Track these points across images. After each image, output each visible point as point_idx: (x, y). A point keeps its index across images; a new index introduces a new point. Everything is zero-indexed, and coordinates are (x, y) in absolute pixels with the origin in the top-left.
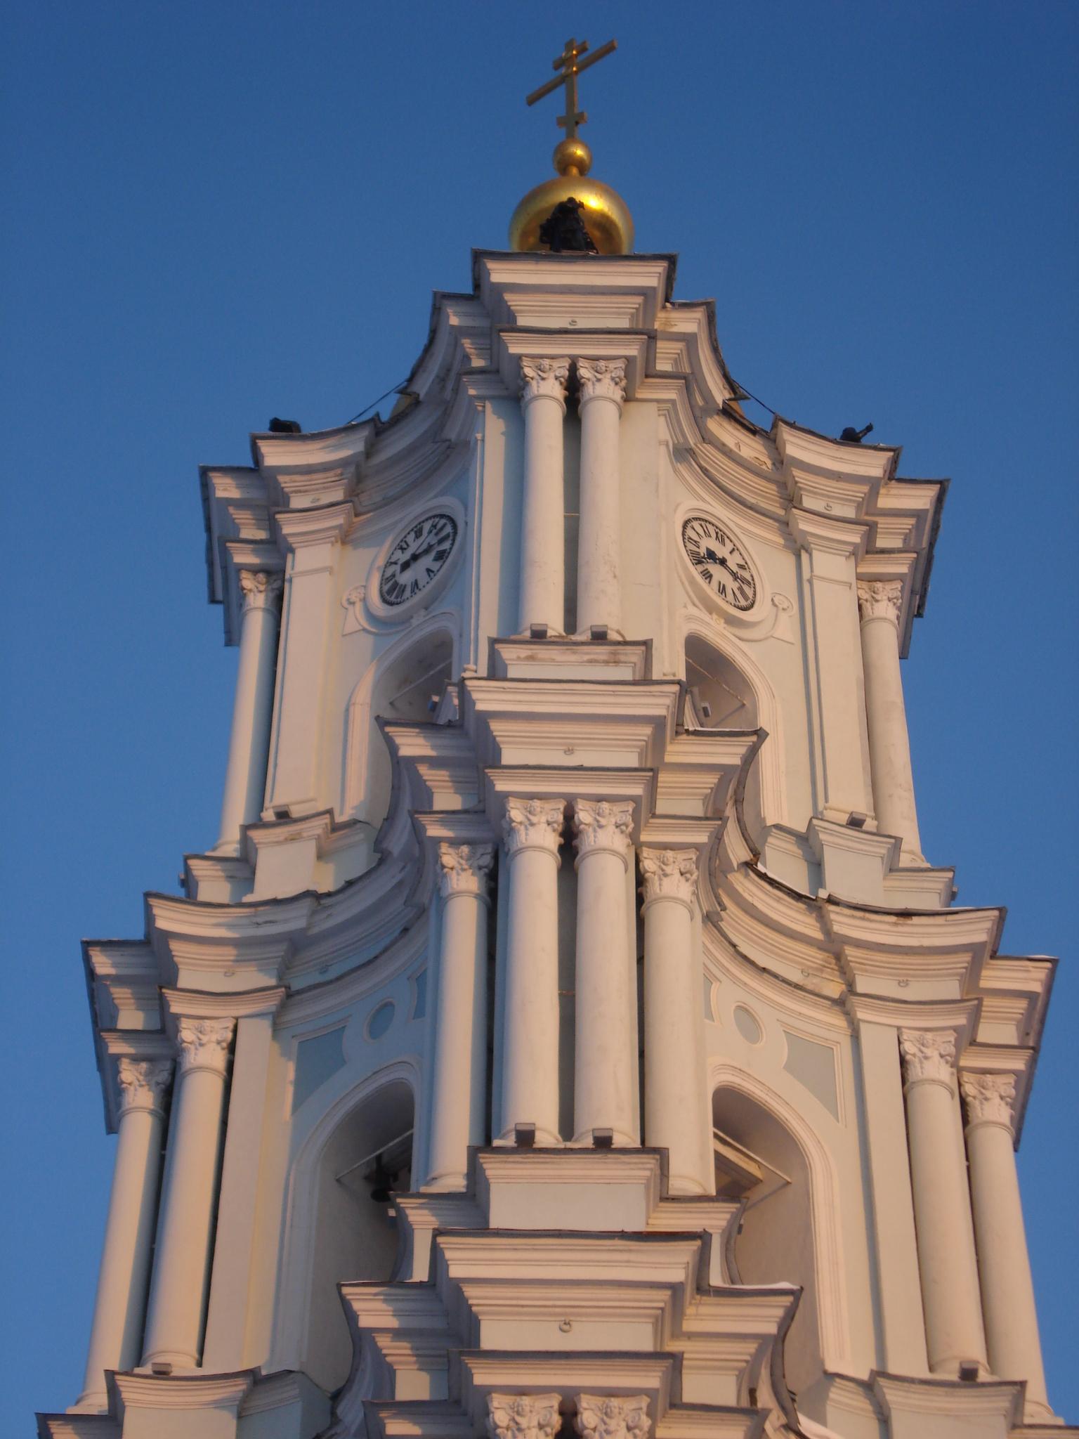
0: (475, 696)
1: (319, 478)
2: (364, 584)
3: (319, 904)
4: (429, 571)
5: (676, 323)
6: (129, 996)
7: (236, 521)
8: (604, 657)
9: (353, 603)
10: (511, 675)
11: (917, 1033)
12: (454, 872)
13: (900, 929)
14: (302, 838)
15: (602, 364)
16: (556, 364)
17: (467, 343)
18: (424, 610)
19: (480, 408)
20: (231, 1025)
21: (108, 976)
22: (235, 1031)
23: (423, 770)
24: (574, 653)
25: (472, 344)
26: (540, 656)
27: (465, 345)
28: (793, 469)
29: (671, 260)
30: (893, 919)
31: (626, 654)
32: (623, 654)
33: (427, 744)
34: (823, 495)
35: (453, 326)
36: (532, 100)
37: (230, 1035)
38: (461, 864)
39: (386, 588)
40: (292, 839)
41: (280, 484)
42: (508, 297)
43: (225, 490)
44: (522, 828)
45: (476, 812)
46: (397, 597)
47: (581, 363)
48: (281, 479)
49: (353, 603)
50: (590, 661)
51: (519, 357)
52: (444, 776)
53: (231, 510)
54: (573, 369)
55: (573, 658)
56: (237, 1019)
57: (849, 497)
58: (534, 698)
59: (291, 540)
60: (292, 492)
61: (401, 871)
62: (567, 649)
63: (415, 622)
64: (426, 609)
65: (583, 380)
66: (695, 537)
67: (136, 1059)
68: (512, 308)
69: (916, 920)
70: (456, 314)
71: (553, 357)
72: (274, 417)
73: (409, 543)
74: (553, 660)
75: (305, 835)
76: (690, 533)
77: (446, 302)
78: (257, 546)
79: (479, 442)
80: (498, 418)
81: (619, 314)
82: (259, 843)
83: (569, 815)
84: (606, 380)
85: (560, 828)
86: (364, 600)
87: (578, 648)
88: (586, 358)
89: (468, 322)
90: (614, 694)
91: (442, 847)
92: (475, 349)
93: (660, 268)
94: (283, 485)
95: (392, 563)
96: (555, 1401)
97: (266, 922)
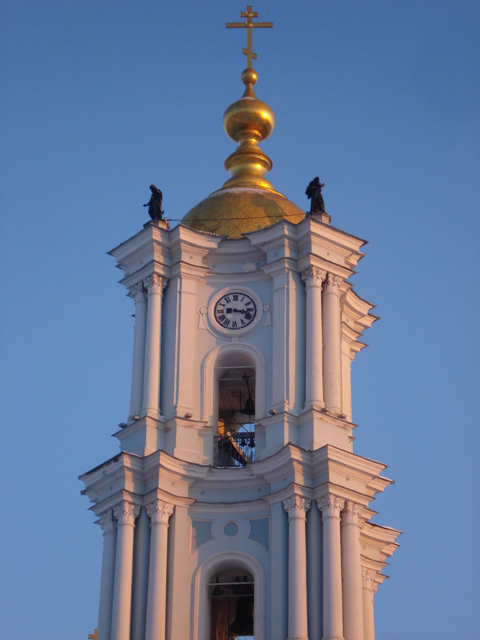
1: (195, 249)
2: (207, 307)
3: (211, 470)
4: (242, 321)
5: (352, 259)
6: (131, 476)
7: (154, 249)
8: (341, 425)
9: (203, 314)
11: (367, 569)
12: (298, 508)
13: (371, 530)
14: (193, 428)
15: (336, 278)
17: (286, 242)
18: (238, 338)
19: (286, 272)
20: (173, 507)
21: (127, 467)
23: (295, 464)
24: (334, 421)
25: (288, 243)
26: (324, 419)
27: (286, 242)
28: (344, 304)
29: (365, 242)
30: (370, 526)
31: (348, 427)
32: (348, 426)
33: (301, 455)
34: (348, 315)
35: (285, 234)
37: (172, 512)
38: (301, 505)
40: (189, 427)
41: (181, 246)
42: (312, 236)
43: (156, 236)
44: (333, 507)
45: (310, 488)
46: (224, 323)
48: (182, 244)
49: (203, 314)
50: (338, 426)
51: (312, 266)
52: (300, 467)
53: (155, 244)
55: (333, 423)
57: (354, 318)
58: (345, 458)
59: (182, 274)
60: (183, 250)
61: (250, 476)
62: (333, 419)
63: (232, 339)
64: (239, 337)
65: (329, 283)
67: (131, 503)
68: (312, 241)
69: (376, 528)
70: (288, 229)
71: (322, 269)
72: (152, 184)
73: (230, 300)
74: (327, 422)
75: (194, 427)
77: (286, 223)
78: (165, 267)
79: (285, 289)
80: (294, 281)
81: (342, 255)
82: (178, 424)
84: (337, 286)
86: (207, 314)
87: (336, 420)
88: (332, 273)
89: (291, 235)
90: (367, 463)
91: (297, 497)
92: (289, 245)
93: (361, 243)
94: (182, 247)
95: (221, 304)
97: (191, 471)
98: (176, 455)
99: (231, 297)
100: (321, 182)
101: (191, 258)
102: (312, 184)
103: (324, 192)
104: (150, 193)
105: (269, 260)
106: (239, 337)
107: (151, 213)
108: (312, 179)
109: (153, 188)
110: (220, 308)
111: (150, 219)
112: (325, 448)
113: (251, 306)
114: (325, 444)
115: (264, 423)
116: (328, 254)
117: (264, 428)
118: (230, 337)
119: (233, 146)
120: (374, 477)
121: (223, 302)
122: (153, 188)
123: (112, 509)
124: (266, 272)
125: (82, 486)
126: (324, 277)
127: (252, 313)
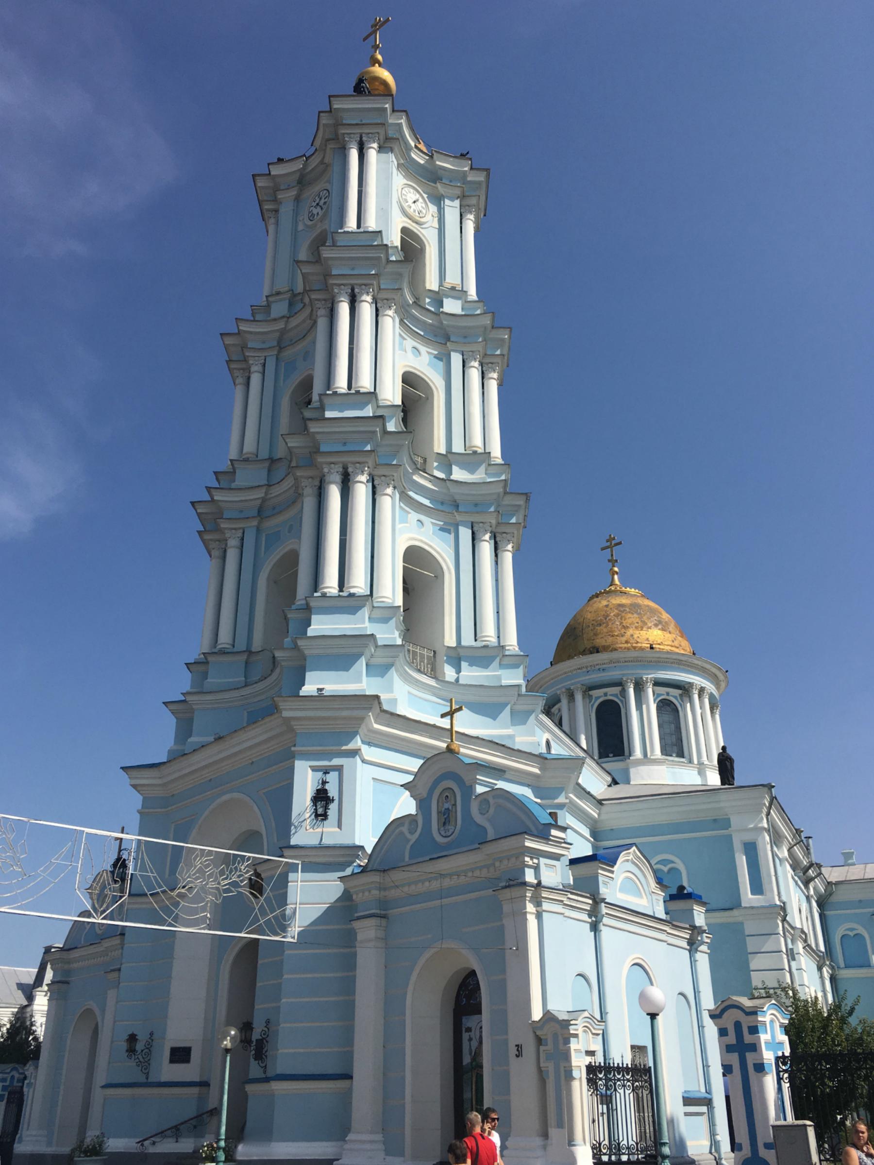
0: (323, 252)
10: (338, 244)
16: (356, 136)
22: (265, 360)
36: (365, 39)
39: (310, 215)
47: (363, 135)
54: (361, 137)
56: (265, 356)
63: (318, 226)
64: (321, 221)
66: (405, 193)
76: (404, 192)
83: (353, 290)
85: (350, 293)
96: (341, 465)
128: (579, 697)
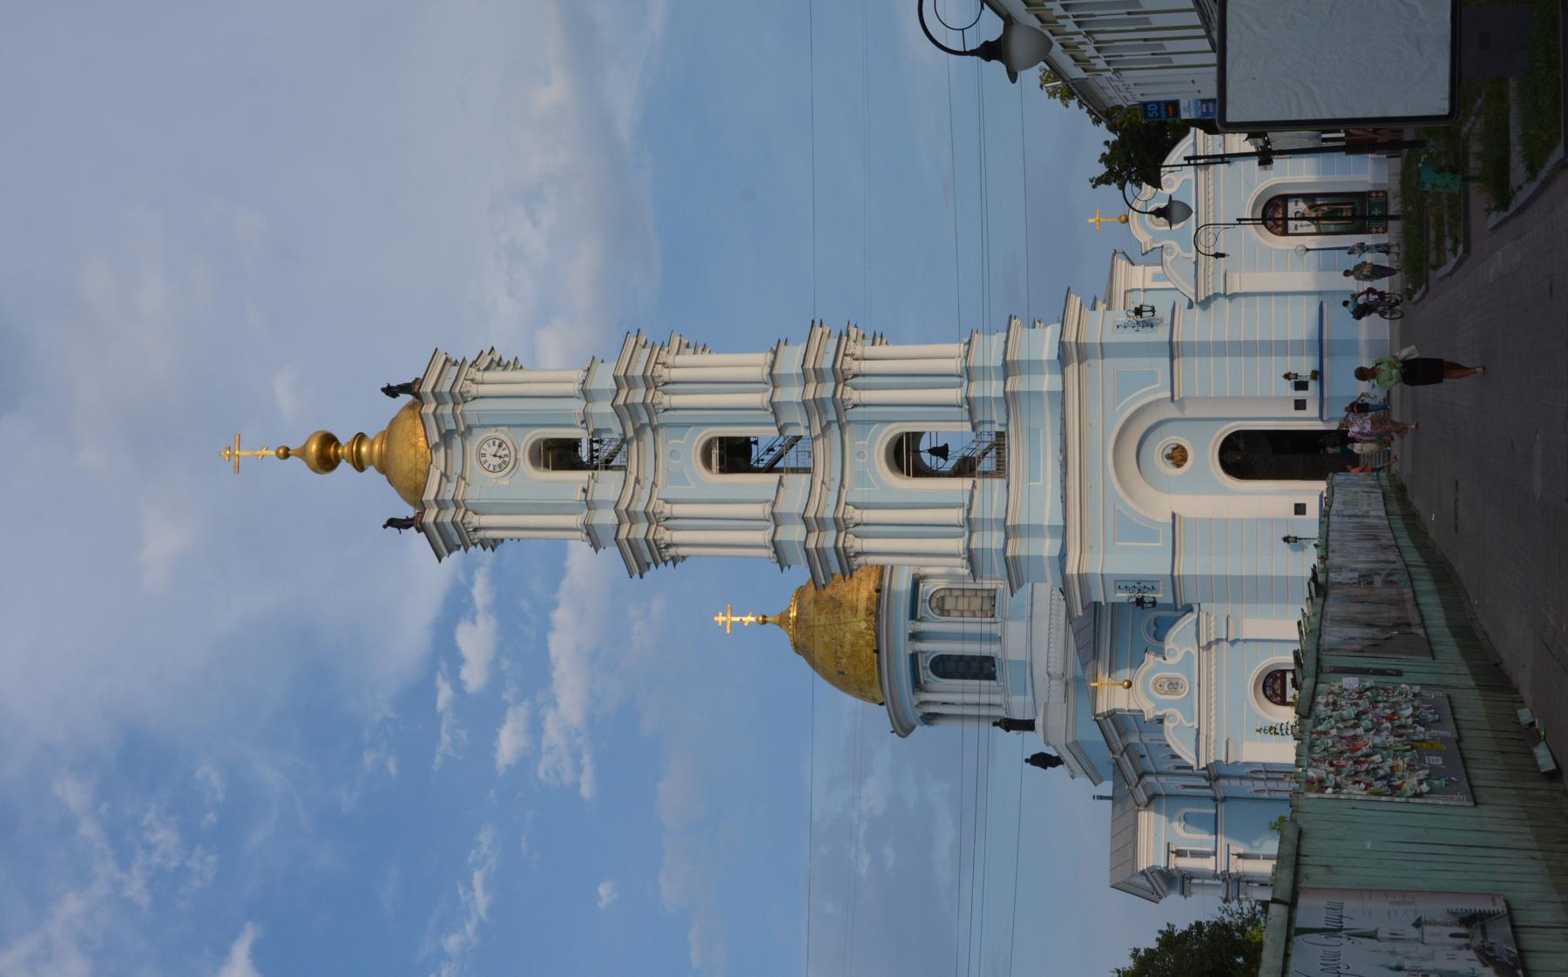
98: (617, 500)
99: (483, 459)
100: (385, 386)
101: (449, 491)
102: (387, 394)
103: (394, 384)
104: (389, 528)
105: (454, 427)
106: (516, 451)
107: (408, 527)
108: (383, 394)
109: (385, 527)
110: (491, 468)
111: (413, 528)
112: (616, 378)
113: (491, 442)
114: (612, 379)
115: (591, 430)
116: (450, 378)
117: (595, 430)
118: (516, 459)
119: (345, 467)
120: (637, 342)
121: (486, 465)
122: (385, 527)
123: (659, 549)
124: (463, 429)
125: (637, 575)
126: (469, 382)
127: (497, 442)
128: (923, 627)
